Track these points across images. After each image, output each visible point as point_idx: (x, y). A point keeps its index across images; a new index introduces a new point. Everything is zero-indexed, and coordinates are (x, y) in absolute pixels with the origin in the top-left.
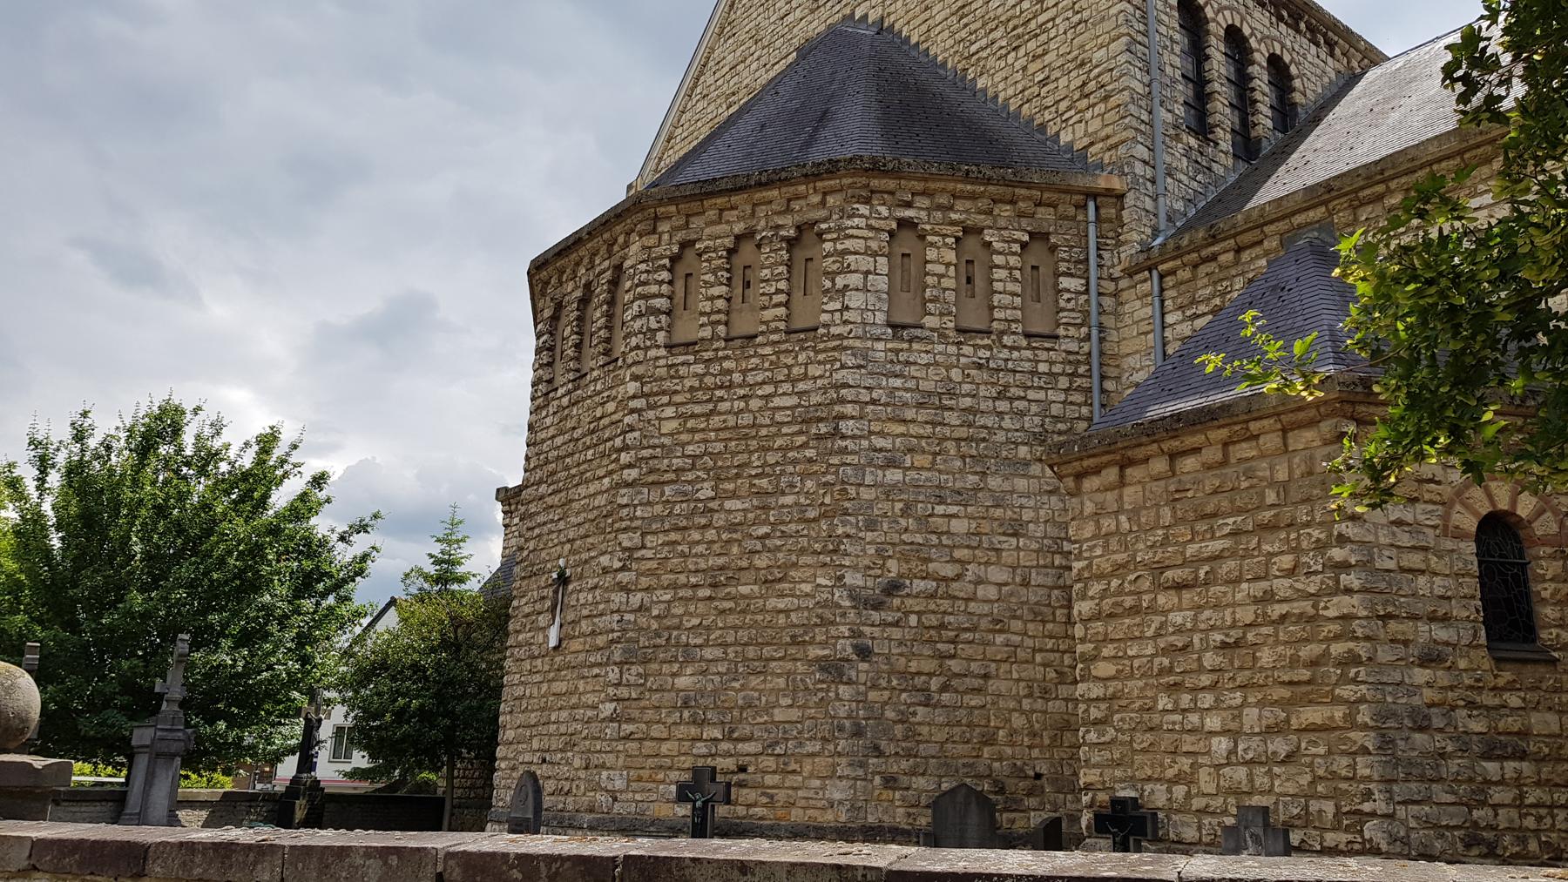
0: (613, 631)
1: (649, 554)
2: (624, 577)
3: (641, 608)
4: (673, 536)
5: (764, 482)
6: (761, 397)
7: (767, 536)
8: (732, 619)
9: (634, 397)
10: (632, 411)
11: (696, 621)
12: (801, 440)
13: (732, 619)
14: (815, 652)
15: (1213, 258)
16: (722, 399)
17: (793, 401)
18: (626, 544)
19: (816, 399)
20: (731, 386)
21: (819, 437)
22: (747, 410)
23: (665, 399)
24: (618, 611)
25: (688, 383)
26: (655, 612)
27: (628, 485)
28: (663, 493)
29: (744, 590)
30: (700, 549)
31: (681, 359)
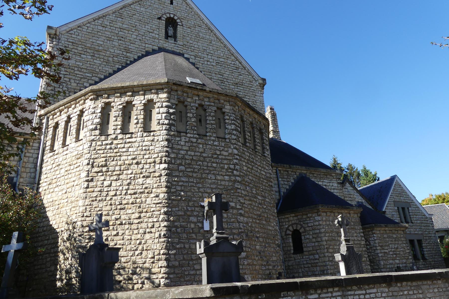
0: (241, 229)
1: (246, 206)
2: (242, 212)
3: (247, 223)
4: (250, 202)
5: (263, 193)
6: (260, 169)
7: (265, 208)
8: (263, 231)
9: (236, 155)
10: (237, 159)
11: (257, 230)
12: (267, 185)
13: (263, 231)
14: (277, 242)
15: (288, 171)
16: (253, 166)
17: (264, 174)
18: (241, 201)
19: (268, 175)
20: (254, 163)
21: (269, 185)
22: (257, 171)
23: (243, 159)
24: (242, 222)
25: (247, 158)
26: (250, 225)
27: (238, 182)
28: (246, 188)
29: (264, 222)
30: (255, 208)
31: (245, 149)
